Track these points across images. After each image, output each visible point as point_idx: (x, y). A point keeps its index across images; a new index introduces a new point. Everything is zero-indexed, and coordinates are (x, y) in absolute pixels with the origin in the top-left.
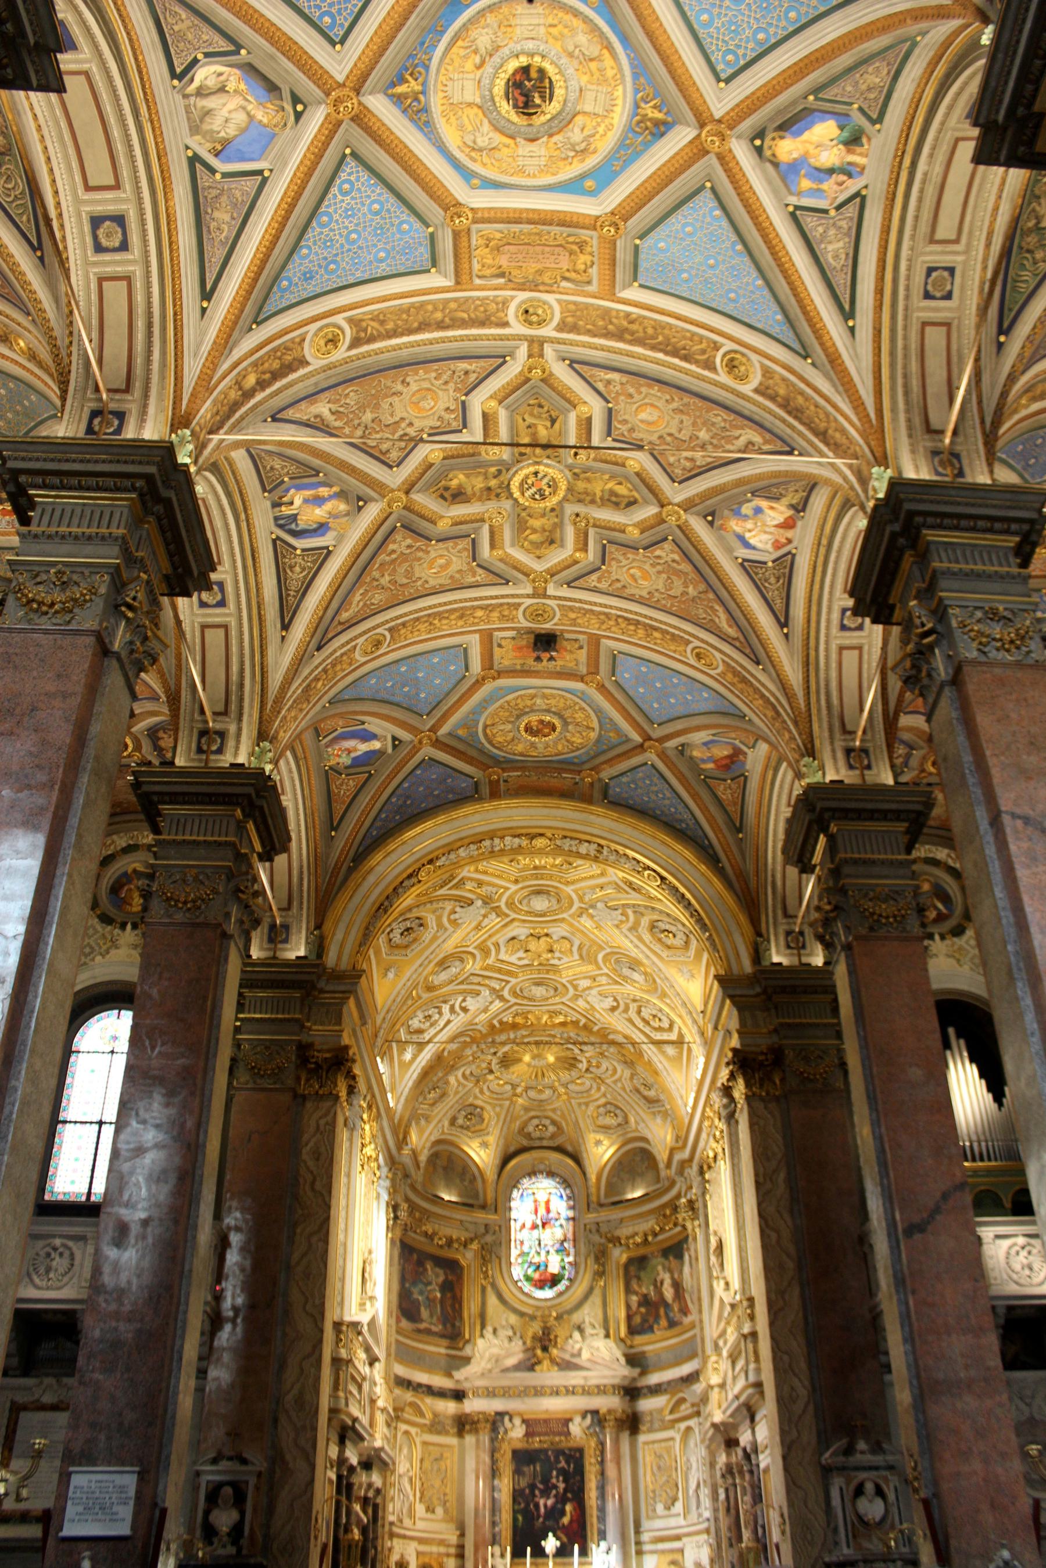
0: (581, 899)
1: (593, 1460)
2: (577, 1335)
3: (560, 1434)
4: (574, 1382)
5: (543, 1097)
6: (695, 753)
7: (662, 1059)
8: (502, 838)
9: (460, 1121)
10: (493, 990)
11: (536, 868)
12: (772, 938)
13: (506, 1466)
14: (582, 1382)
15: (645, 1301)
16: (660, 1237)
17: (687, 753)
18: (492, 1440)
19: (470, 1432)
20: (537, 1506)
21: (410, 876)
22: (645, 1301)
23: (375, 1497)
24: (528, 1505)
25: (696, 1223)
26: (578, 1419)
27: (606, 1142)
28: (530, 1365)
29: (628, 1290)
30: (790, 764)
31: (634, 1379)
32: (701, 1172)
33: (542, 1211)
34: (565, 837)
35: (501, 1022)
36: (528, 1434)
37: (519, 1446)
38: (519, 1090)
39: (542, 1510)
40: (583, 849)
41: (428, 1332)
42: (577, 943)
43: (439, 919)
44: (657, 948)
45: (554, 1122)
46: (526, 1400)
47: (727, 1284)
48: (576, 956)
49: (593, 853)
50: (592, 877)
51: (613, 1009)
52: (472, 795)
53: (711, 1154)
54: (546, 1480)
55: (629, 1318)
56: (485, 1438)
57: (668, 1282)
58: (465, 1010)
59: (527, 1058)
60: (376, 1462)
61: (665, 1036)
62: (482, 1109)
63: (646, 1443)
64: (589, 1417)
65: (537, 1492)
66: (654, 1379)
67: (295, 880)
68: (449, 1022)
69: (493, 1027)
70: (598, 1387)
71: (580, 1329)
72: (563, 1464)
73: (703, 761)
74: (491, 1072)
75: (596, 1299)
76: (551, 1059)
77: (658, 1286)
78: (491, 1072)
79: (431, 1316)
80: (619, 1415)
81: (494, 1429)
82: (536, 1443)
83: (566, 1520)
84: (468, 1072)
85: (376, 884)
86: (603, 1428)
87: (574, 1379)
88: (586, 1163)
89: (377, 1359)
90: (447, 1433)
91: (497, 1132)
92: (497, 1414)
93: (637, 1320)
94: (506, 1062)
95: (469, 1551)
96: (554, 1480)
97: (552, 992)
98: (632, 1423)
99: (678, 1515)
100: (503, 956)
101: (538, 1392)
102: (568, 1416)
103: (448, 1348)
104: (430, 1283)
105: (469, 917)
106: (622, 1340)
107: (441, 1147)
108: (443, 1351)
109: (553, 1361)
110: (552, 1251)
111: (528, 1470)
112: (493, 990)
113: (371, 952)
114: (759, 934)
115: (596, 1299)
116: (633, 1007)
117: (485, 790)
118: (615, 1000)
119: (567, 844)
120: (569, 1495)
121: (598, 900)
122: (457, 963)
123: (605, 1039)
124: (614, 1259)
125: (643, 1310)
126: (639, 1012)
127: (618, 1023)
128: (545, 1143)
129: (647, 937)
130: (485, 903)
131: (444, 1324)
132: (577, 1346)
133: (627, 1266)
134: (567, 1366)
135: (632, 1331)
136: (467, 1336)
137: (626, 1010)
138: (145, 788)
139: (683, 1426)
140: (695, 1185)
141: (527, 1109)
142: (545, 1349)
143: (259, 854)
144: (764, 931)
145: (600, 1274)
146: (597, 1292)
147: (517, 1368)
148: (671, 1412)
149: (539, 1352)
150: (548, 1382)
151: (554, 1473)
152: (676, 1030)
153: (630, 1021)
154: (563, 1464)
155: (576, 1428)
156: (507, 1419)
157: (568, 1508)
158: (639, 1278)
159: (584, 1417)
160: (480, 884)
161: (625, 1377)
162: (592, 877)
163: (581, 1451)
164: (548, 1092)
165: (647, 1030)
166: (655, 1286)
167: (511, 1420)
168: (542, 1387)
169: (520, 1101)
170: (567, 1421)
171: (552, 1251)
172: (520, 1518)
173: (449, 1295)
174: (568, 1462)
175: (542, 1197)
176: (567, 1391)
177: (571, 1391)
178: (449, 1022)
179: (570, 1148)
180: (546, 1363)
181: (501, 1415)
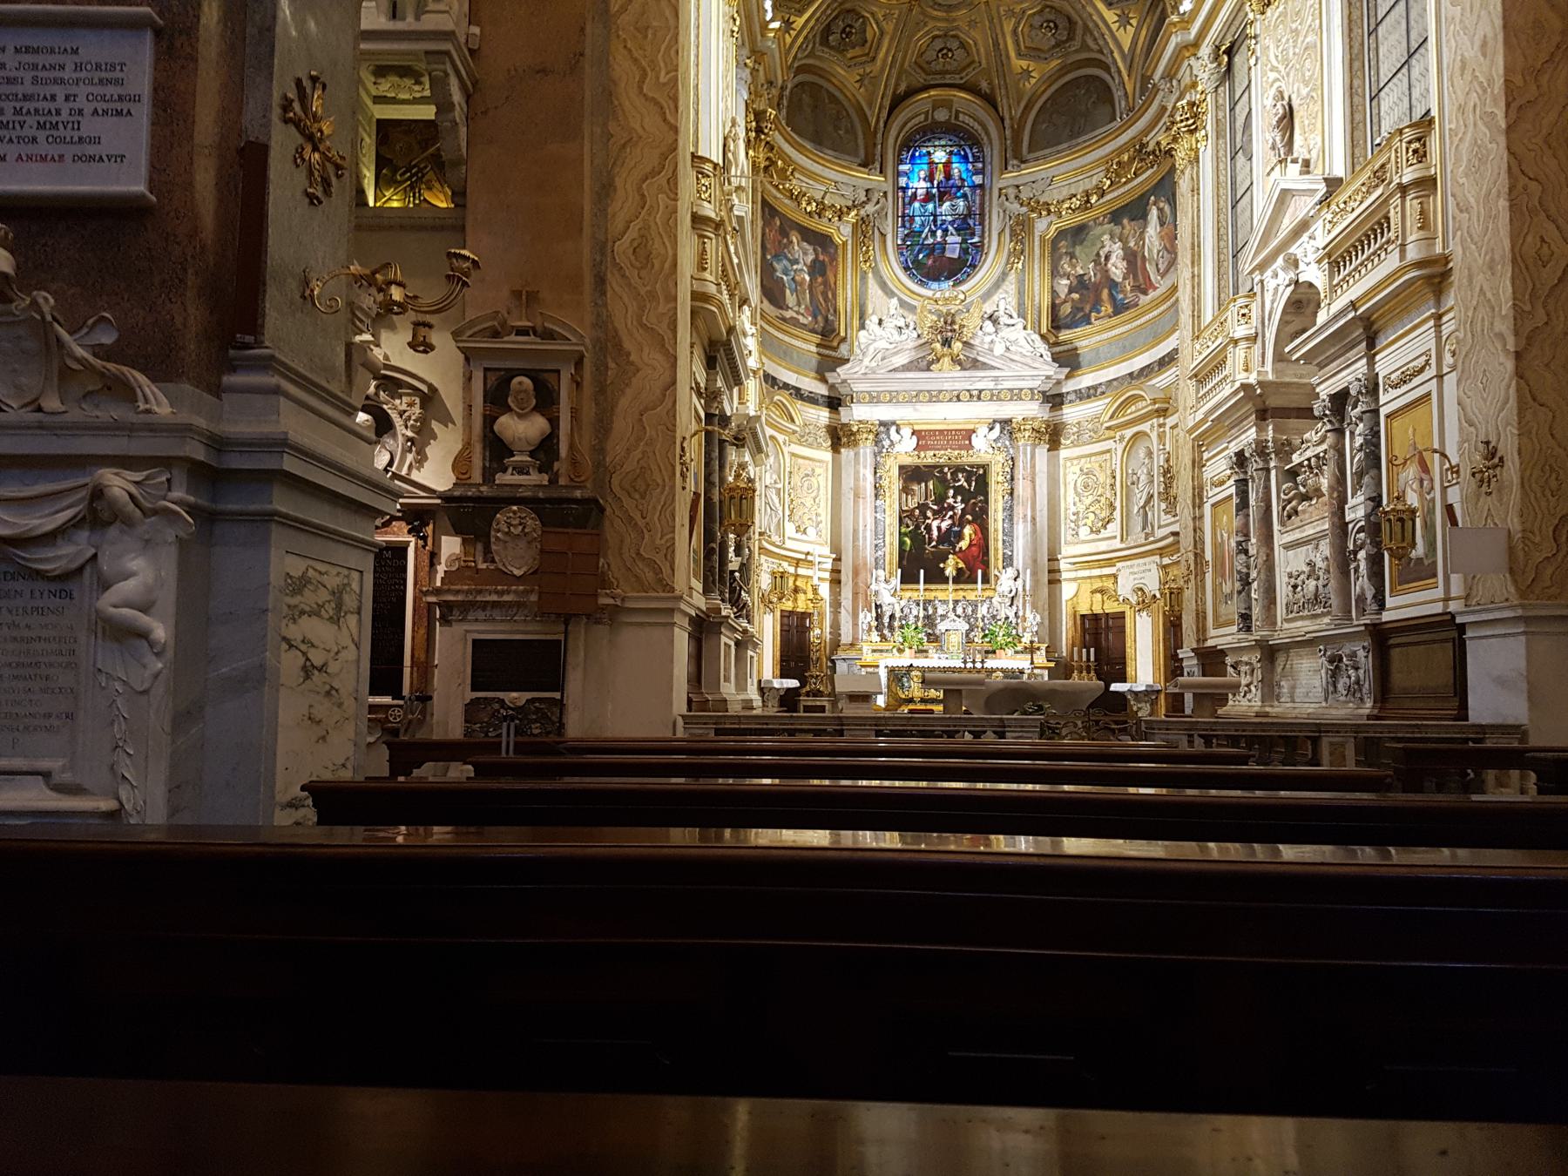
1: (1000, 479)
4: (980, 386)
13: (893, 482)
14: (991, 385)
19: (848, 445)
20: (929, 528)
24: (917, 527)
26: (982, 430)
28: (924, 363)
29: (1055, 273)
31: (1059, 383)
36: (918, 448)
37: (908, 461)
39: (935, 533)
41: (794, 322)
46: (918, 406)
54: (940, 500)
55: (1054, 308)
63: (1071, 459)
65: (929, 514)
66: (1085, 380)
70: (1011, 390)
71: (992, 318)
72: (963, 482)
75: (1010, 285)
80: (1036, 425)
82: (928, 458)
83: (964, 544)
87: (981, 381)
90: (819, 446)
92: (882, 424)
93: (1066, 309)
96: (951, 501)
98: (1053, 436)
99: (1115, 537)
101: (934, 397)
102: (971, 427)
103: (818, 345)
108: (813, 349)
109: (956, 361)
115: (1010, 285)
124: (1037, 234)
125: (1076, 296)
131: (815, 317)
135: (1057, 324)
136: (843, 334)
146: (1012, 277)
147: (906, 368)
150: (947, 386)
151: (951, 492)
154: (963, 482)
155: (979, 442)
156: (893, 429)
157: (968, 530)
159: (991, 429)
161: (1048, 377)
163: (985, 467)
167: (898, 432)
172: (908, 541)
173: (820, 280)
174: (968, 481)
176: (971, 396)
177: (978, 396)
180: (947, 360)
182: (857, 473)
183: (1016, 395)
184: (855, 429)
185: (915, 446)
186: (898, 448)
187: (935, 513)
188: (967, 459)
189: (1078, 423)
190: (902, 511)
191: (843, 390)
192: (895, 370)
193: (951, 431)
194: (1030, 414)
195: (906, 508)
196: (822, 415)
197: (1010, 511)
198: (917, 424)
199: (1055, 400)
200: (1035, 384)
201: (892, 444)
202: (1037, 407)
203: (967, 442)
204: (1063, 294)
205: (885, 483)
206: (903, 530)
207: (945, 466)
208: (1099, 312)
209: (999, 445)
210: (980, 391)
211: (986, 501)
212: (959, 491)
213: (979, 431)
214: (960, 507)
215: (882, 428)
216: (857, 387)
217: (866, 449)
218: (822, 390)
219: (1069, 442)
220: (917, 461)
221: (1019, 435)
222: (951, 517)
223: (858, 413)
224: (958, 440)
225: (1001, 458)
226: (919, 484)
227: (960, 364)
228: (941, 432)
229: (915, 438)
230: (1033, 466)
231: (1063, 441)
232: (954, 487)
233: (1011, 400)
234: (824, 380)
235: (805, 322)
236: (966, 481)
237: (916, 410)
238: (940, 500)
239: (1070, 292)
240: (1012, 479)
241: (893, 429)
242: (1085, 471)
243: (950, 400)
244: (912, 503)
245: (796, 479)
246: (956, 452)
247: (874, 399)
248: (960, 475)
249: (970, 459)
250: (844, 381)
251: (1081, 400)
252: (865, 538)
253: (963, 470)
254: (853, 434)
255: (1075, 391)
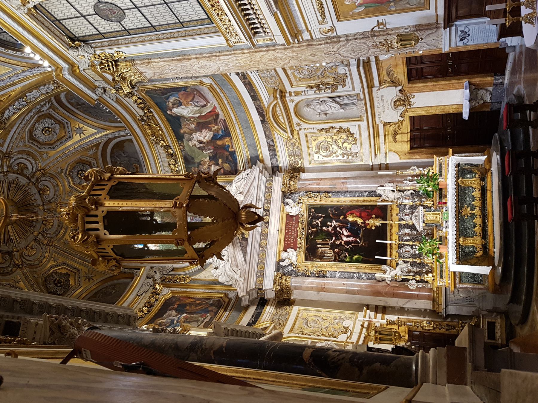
1: (318, 199)
19: (289, 294)
26: (288, 209)
37: (302, 255)
56: (293, 281)
82: (302, 242)
90: (289, 314)
93: (227, 166)
95: (380, 301)
102: (285, 216)
103: (225, 310)
108: (226, 314)
131: (208, 312)
147: (245, 254)
156: (282, 264)
159: (288, 204)
170: (289, 217)
181: (279, 268)
185: (293, 250)
186: (294, 260)
189: (289, 156)
191: (254, 295)
193: (286, 228)
194: (280, 184)
196: (269, 310)
198: (280, 248)
199: (275, 170)
201: (291, 264)
202: (277, 178)
203: (294, 218)
207: (308, 231)
209: (297, 200)
213: (288, 211)
215: (281, 271)
216: (253, 284)
217: (293, 281)
218: (252, 310)
219: (300, 162)
220: (303, 249)
221: (292, 188)
223: (268, 284)
224: (292, 224)
228: (286, 234)
229: (288, 250)
230: (312, 180)
231: (299, 165)
234: (246, 308)
235: (209, 318)
236: (318, 220)
237: (271, 248)
241: (282, 264)
242: (317, 150)
243: (267, 227)
245: (308, 330)
246: (300, 225)
247: (261, 274)
248: (314, 223)
249: (305, 216)
250: (248, 293)
251: (276, 155)
254: (282, 290)
255: (271, 159)
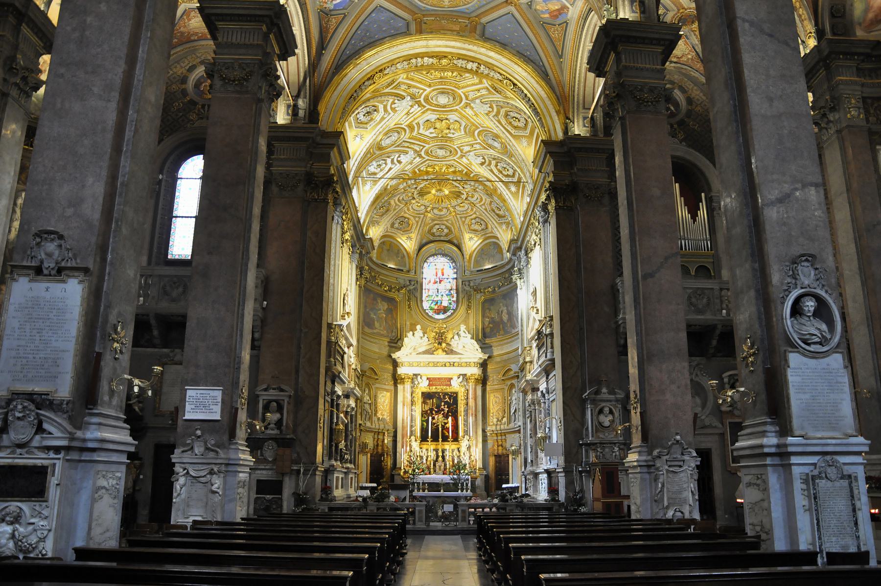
0: (467, 99)
1: (463, 398)
2: (456, 337)
3: (447, 385)
5: (442, 213)
6: (538, 7)
7: (508, 192)
8: (422, 58)
9: (396, 225)
10: (415, 151)
11: (441, 78)
12: (576, 120)
13: (419, 399)
14: (458, 360)
15: (492, 321)
16: (502, 289)
17: (533, 7)
18: (412, 387)
19: (400, 383)
21: (369, 79)
22: (492, 321)
23: (351, 412)
25: (522, 280)
26: (455, 378)
27: (476, 239)
29: (483, 316)
30: (596, 13)
32: (527, 254)
33: (440, 274)
34: (459, 59)
35: (419, 170)
36: (429, 385)
37: (425, 390)
38: (429, 209)
40: (470, 66)
42: (463, 124)
43: (385, 107)
44: (509, 128)
45: (447, 227)
47: (538, 310)
48: (463, 133)
49: (474, 69)
50: (473, 85)
51: (482, 164)
52: (405, 32)
53: (533, 243)
54: (438, 407)
55: (483, 329)
57: (505, 311)
58: (399, 162)
59: (433, 191)
60: (351, 395)
61: (510, 180)
62: (409, 219)
64: (461, 377)
65: (434, 412)
67: (302, 79)
68: (390, 169)
69: (415, 173)
72: (447, 399)
73: (543, 12)
74: (414, 198)
76: (447, 192)
77: (500, 314)
78: (414, 198)
79: (380, 326)
80: (476, 377)
81: (413, 382)
82: (433, 389)
84: (401, 198)
85: (349, 83)
86: (468, 382)
88: (464, 249)
89: (352, 345)
91: (416, 232)
92: (414, 375)
94: (422, 193)
96: (443, 407)
97: (449, 153)
100: (421, 131)
101: (435, 364)
103: (389, 342)
104: (380, 310)
105: (404, 106)
106: (480, 340)
107: (385, 239)
109: (444, 350)
110: (444, 295)
111: (430, 402)
112: (415, 151)
113: (347, 124)
114: (568, 118)
116: (494, 163)
117: (413, 27)
118: (484, 158)
119: (460, 63)
120: (450, 414)
121: (476, 98)
122: (396, 134)
123: (477, 180)
125: (491, 325)
126: (496, 166)
127: (483, 172)
128: (442, 238)
129: (503, 122)
130: (412, 98)
132: (457, 342)
133: (483, 303)
134: (450, 351)
135: (485, 336)
136: (399, 337)
137: (490, 164)
138: (207, 11)
139: (509, 383)
140: (523, 260)
141: (433, 220)
142: (440, 344)
143: (278, 55)
144: (571, 117)
145: (469, 307)
148: (503, 375)
149: (436, 345)
152: (517, 175)
153: (491, 171)
154: (447, 399)
156: (419, 377)
158: (490, 310)
159: (459, 378)
160: (409, 86)
162: (473, 85)
163: (456, 393)
164: (445, 211)
165: (500, 176)
166: (498, 314)
168: (438, 362)
169: (429, 215)
171: (444, 295)
173: (390, 316)
175: (440, 266)
176: (450, 364)
177: (453, 365)
178: (390, 169)
179: (455, 241)
180: (440, 351)
181: (416, 375)
182: (404, 395)
183: (468, 364)
184: (403, 377)
186: (421, 385)
187: (436, 412)
188: (449, 390)
190: (422, 411)
192: (420, 353)
194: (473, 373)
195: (424, 410)
197: (466, 411)
200: (476, 360)
204: (487, 324)
205: (416, 399)
206: (423, 419)
208: (499, 333)
210: (454, 363)
211: (457, 407)
212: (446, 403)
214: (446, 409)
217: (408, 385)
222: (443, 414)
225: (463, 389)
226: (430, 400)
227: (446, 351)
229: (428, 381)
232: (444, 402)
233: (466, 366)
238: (438, 407)
239: (489, 324)
240: (467, 398)
243: (442, 366)
244: (427, 408)
246: (445, 387)
247: (411, 365)
252: (407, 423)
253: (448, 394)
